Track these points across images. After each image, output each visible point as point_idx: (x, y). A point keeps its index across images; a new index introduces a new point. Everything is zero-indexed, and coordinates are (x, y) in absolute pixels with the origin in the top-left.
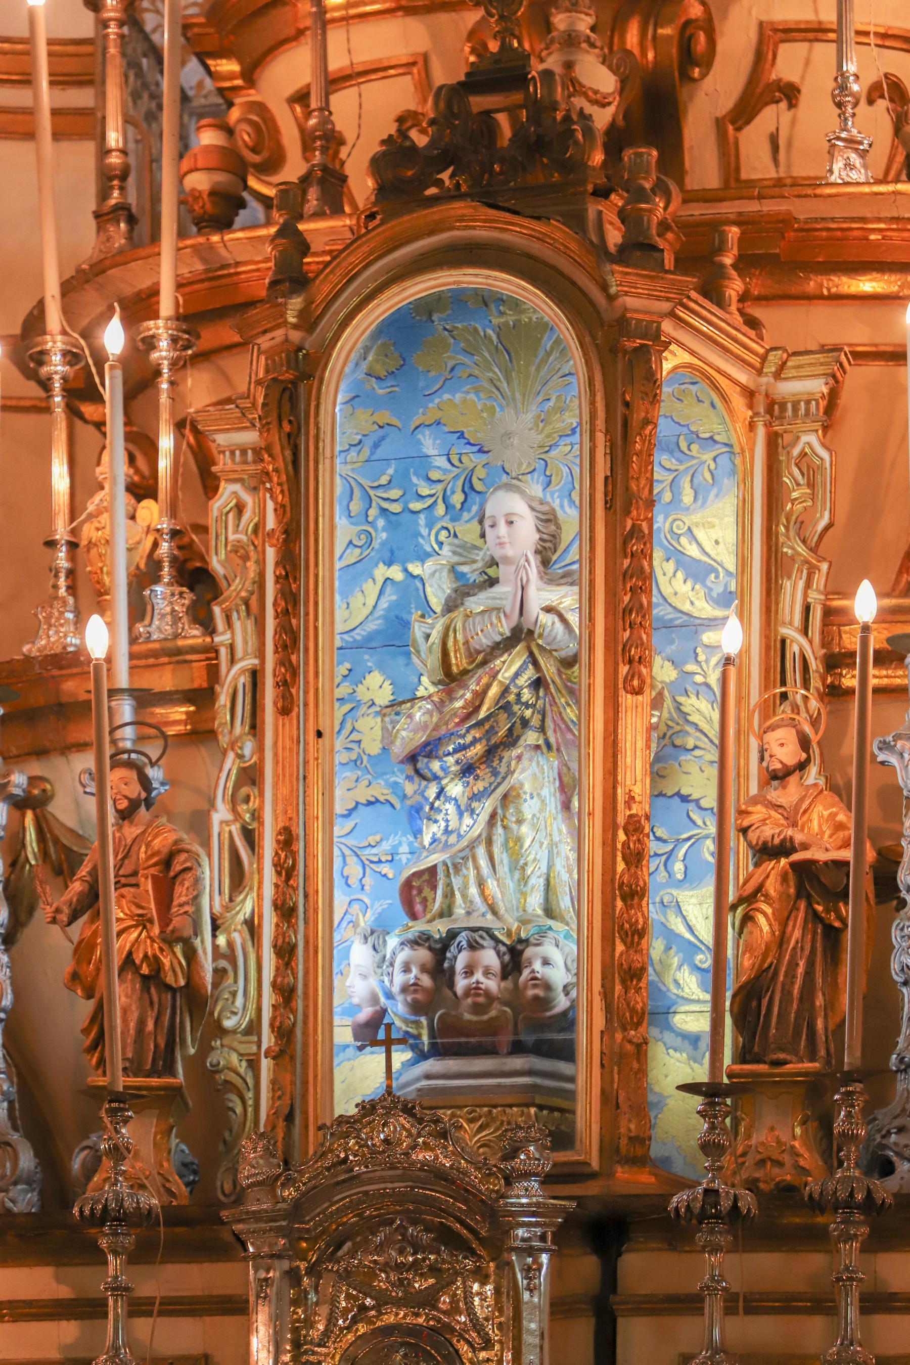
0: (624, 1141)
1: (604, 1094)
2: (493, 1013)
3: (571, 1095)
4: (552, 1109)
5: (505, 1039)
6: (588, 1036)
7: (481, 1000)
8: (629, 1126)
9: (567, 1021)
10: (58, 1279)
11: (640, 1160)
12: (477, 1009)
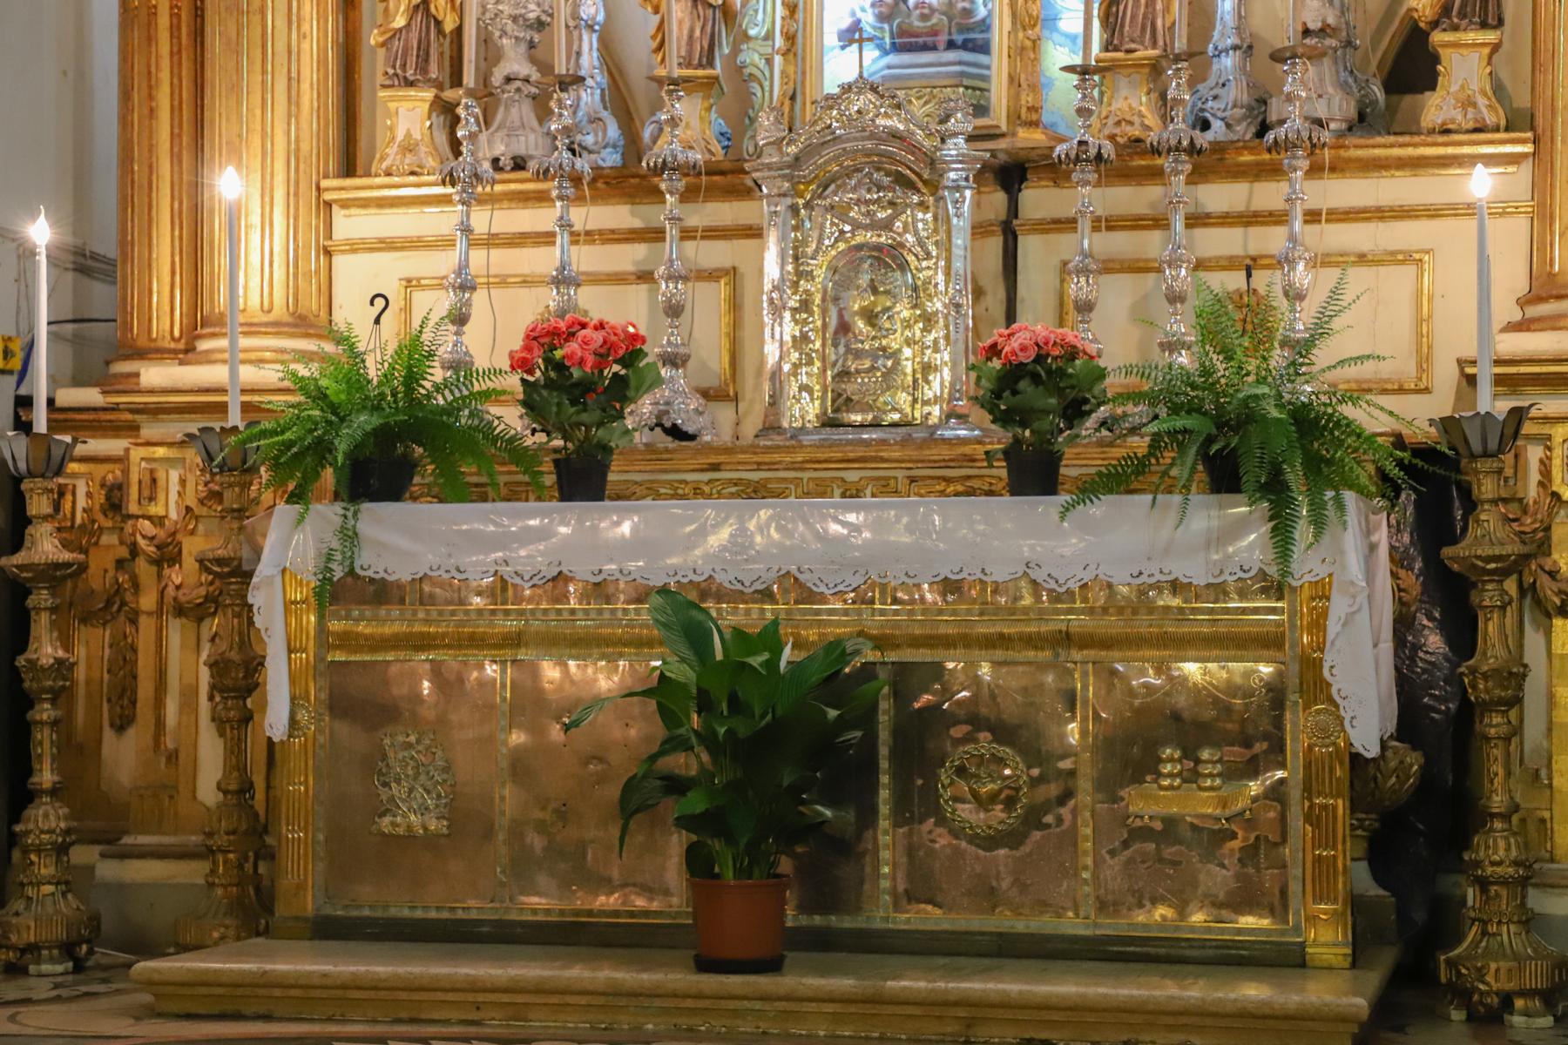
0: (1024, 110)
1: (1011, 78)
2: (934, 21)
3: (986, 79)
4: (974, 89)
5: (943, 38)
6: (1000, 36)
7: (926, 11)
8: (1027, 99)
9: (985, 26)
10: (633, 214)
11: (1034, 124)
12: (924, 17)
